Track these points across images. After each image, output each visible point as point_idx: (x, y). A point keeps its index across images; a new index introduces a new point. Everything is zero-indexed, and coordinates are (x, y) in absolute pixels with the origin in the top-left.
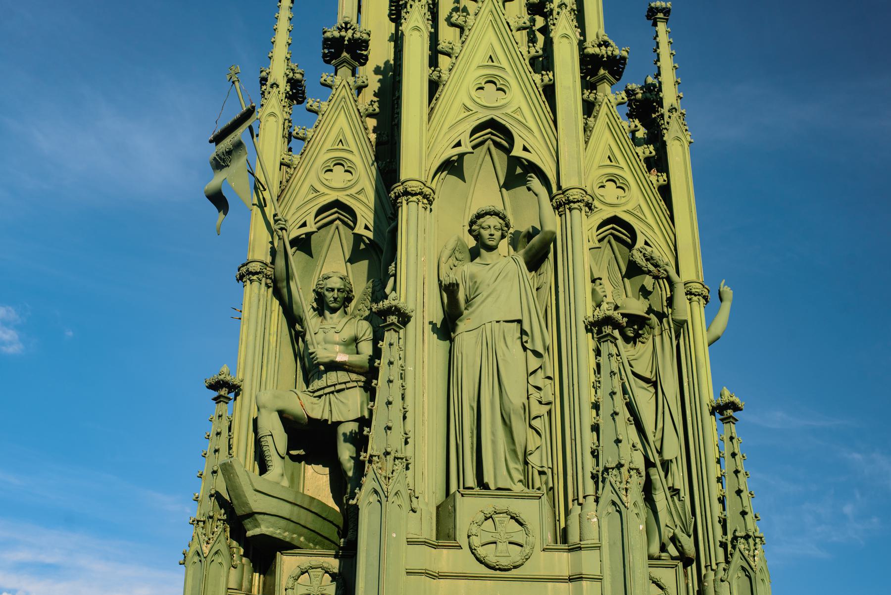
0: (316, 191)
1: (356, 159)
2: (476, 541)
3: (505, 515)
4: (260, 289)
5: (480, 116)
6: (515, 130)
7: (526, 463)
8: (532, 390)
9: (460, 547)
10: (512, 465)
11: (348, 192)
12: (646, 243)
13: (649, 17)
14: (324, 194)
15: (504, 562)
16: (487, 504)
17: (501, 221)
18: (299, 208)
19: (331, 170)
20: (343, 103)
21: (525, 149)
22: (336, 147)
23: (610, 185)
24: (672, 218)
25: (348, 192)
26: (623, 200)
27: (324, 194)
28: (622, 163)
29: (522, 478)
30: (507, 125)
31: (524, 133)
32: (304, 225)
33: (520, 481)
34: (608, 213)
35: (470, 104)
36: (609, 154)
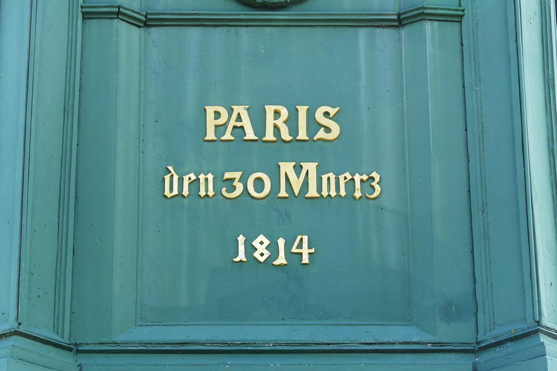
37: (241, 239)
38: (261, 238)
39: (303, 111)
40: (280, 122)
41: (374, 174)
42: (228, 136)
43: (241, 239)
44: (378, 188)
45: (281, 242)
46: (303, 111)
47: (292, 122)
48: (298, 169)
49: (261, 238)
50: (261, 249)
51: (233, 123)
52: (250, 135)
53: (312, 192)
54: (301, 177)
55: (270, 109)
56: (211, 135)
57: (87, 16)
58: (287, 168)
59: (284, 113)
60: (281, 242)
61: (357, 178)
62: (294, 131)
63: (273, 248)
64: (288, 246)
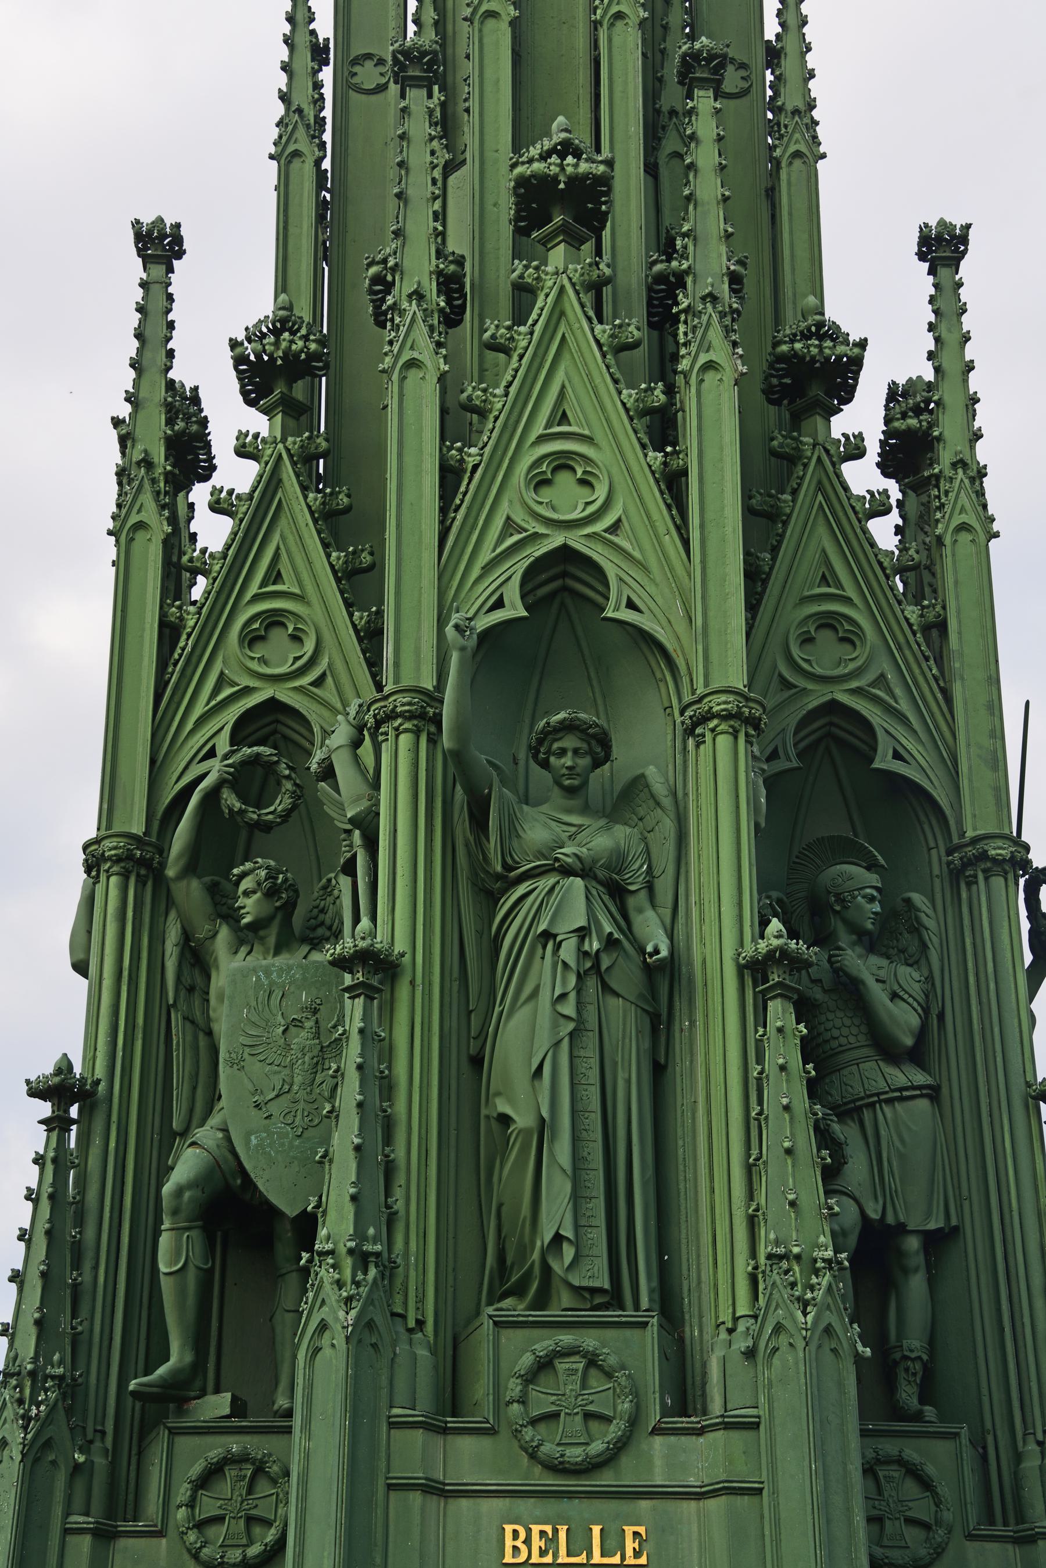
0: (234, 684)
1: (312, 613)
3: (576, 1358)
11: (297, 683)
12: (897, 756)
13: (922, 256)
14: (247, 691)
15: (575, 1454)
19: (262, 638)
20: (279, 494)
22: (271, 588)
24: (949, 699)
25: (297, 683)
26: (852, 666)
27: (247, 691)
36: (823, 569)
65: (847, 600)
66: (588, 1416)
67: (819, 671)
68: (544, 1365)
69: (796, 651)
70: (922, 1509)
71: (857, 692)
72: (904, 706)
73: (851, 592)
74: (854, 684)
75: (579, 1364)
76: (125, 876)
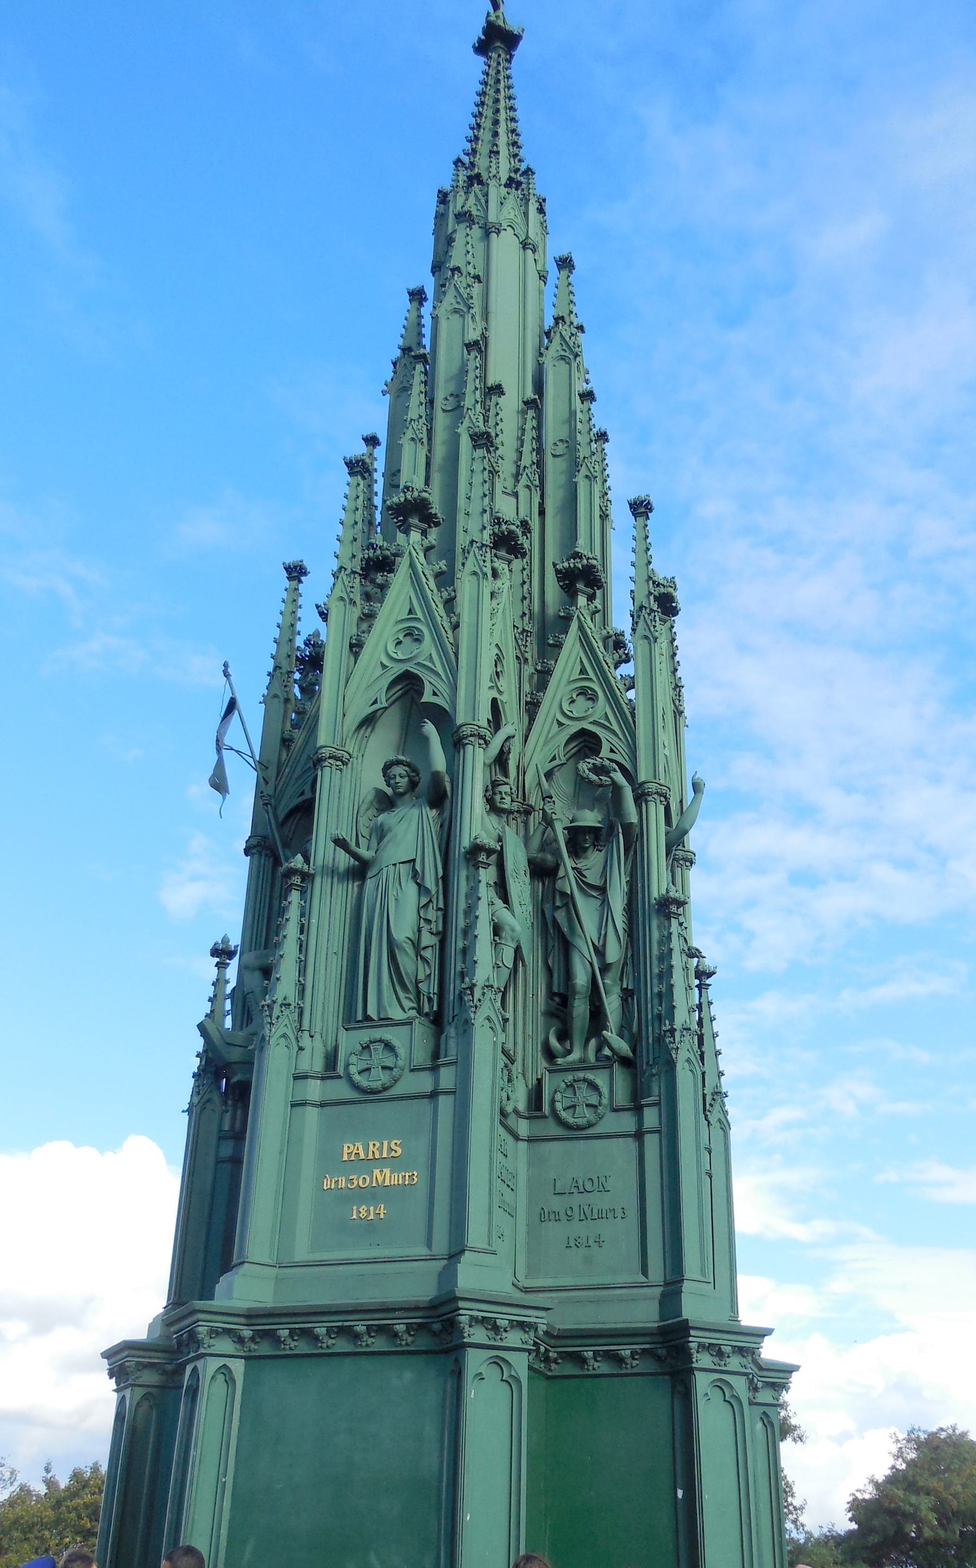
2: (353, 1069)
4: (260, 862)
5: (396, 670)
6: (426, 677)
7: (418, 992)
8: (422, 923)
9: (340, 1077)
10: (402, 995)
16: (365, 1035)
17: (406, 768)
18: (297, 779)
21: (435, 694)
23: (581, 699)
28: (592, 675)
29: (415, 1005)
30: (419, 674)
31: (433, 678)
32: (302, 793)
33: (413, 1008)
34: (575, 727)
35: (386, 662)
37: (355, 1208)
38: (364, 1207)
39: (385, 1143)
40: (375, 1150)
41: (416, 1173)
42: (353, 1158)
43: (355, 1208)
44: (416, 1179)
45: (372, 1208)
46: (385, 1143)
47: (381, 1149)
48: (381, 1171)
49: (364, 1207)
50: (363, 1212)
51: (355, 1151)
52: (362, 1156)
53: (387, 1183)
54: (386, 1176)
55: (371, 1144)
56: (345, 1158)
57: (292, 1106)
58: (376, 1172)
59: (378, 1145)
60: (372, 1208)
61: (407, 1174)
62: (381, 1153)
63: (368, 1211)
64: (375, 1210)
65: (591, 679)
66: (384, 1068)
67: (576, 715)
68: (366, 1048)
69: (566, 707)
70: (594, 1100)
71: (595, 723)
72: (615, 727)
73: (592, 675)
74: (591, 720)
75: (380, 1047)
76: (260, 854)
